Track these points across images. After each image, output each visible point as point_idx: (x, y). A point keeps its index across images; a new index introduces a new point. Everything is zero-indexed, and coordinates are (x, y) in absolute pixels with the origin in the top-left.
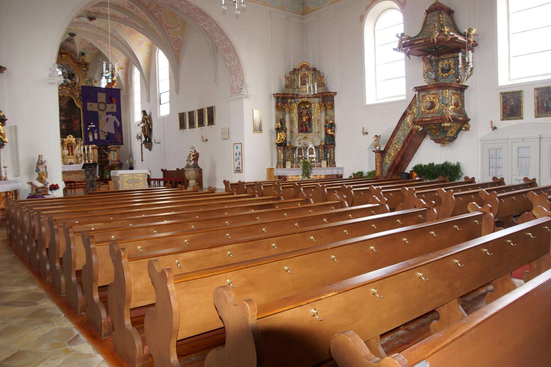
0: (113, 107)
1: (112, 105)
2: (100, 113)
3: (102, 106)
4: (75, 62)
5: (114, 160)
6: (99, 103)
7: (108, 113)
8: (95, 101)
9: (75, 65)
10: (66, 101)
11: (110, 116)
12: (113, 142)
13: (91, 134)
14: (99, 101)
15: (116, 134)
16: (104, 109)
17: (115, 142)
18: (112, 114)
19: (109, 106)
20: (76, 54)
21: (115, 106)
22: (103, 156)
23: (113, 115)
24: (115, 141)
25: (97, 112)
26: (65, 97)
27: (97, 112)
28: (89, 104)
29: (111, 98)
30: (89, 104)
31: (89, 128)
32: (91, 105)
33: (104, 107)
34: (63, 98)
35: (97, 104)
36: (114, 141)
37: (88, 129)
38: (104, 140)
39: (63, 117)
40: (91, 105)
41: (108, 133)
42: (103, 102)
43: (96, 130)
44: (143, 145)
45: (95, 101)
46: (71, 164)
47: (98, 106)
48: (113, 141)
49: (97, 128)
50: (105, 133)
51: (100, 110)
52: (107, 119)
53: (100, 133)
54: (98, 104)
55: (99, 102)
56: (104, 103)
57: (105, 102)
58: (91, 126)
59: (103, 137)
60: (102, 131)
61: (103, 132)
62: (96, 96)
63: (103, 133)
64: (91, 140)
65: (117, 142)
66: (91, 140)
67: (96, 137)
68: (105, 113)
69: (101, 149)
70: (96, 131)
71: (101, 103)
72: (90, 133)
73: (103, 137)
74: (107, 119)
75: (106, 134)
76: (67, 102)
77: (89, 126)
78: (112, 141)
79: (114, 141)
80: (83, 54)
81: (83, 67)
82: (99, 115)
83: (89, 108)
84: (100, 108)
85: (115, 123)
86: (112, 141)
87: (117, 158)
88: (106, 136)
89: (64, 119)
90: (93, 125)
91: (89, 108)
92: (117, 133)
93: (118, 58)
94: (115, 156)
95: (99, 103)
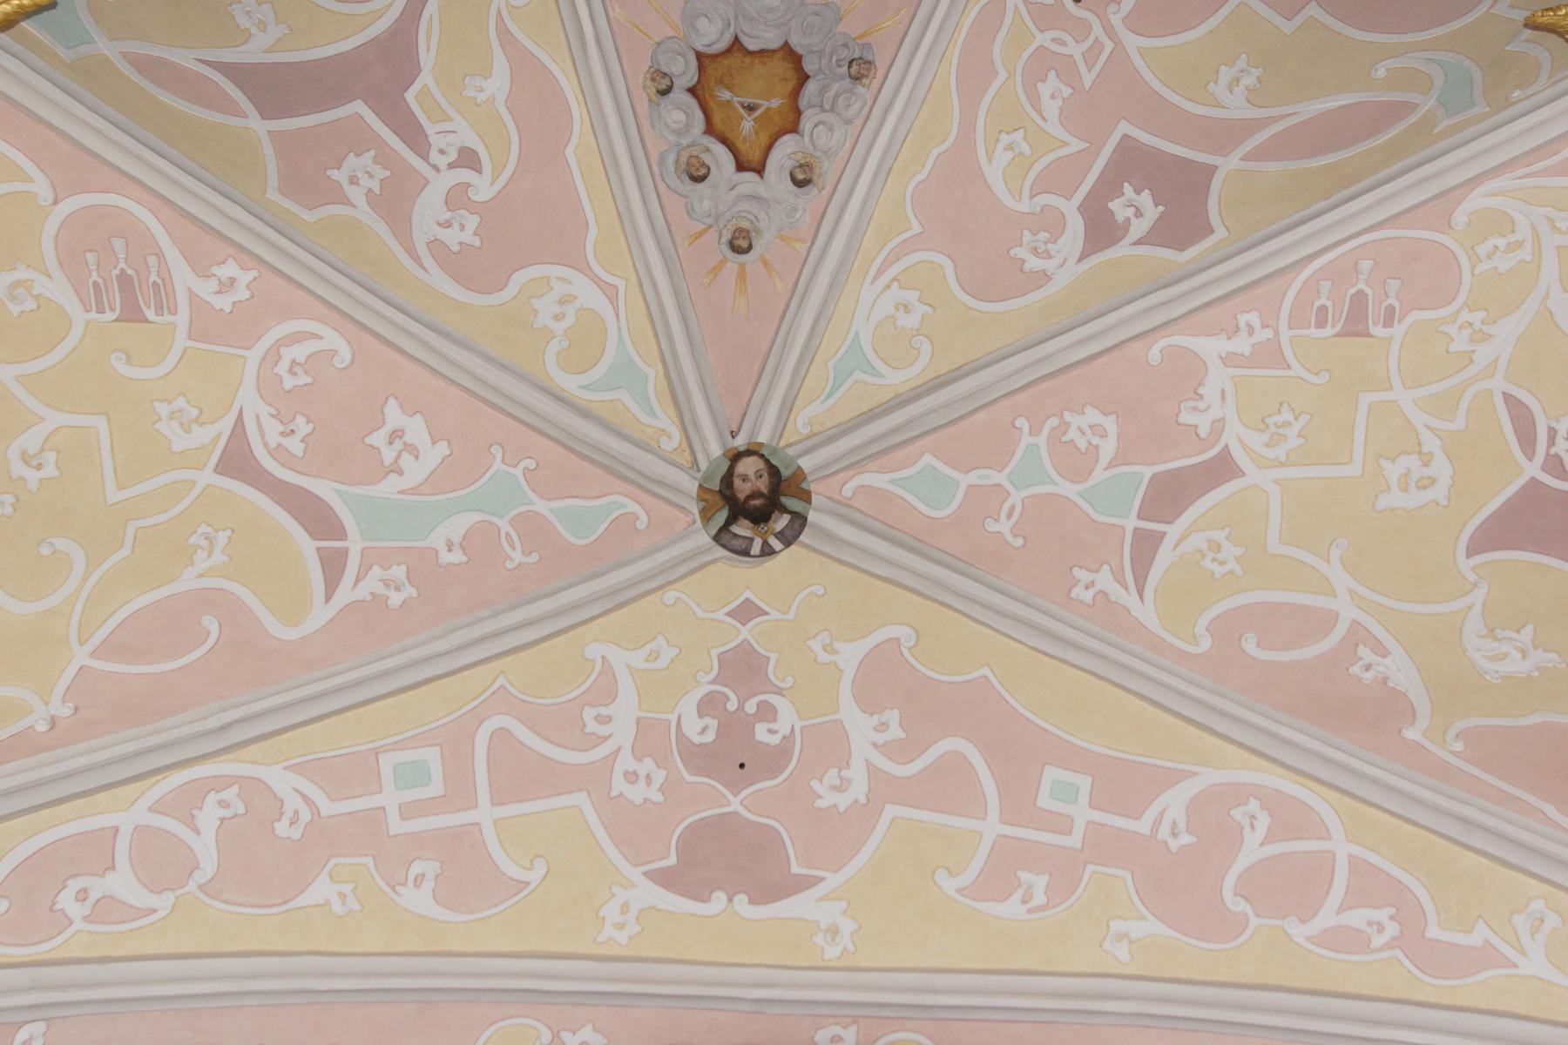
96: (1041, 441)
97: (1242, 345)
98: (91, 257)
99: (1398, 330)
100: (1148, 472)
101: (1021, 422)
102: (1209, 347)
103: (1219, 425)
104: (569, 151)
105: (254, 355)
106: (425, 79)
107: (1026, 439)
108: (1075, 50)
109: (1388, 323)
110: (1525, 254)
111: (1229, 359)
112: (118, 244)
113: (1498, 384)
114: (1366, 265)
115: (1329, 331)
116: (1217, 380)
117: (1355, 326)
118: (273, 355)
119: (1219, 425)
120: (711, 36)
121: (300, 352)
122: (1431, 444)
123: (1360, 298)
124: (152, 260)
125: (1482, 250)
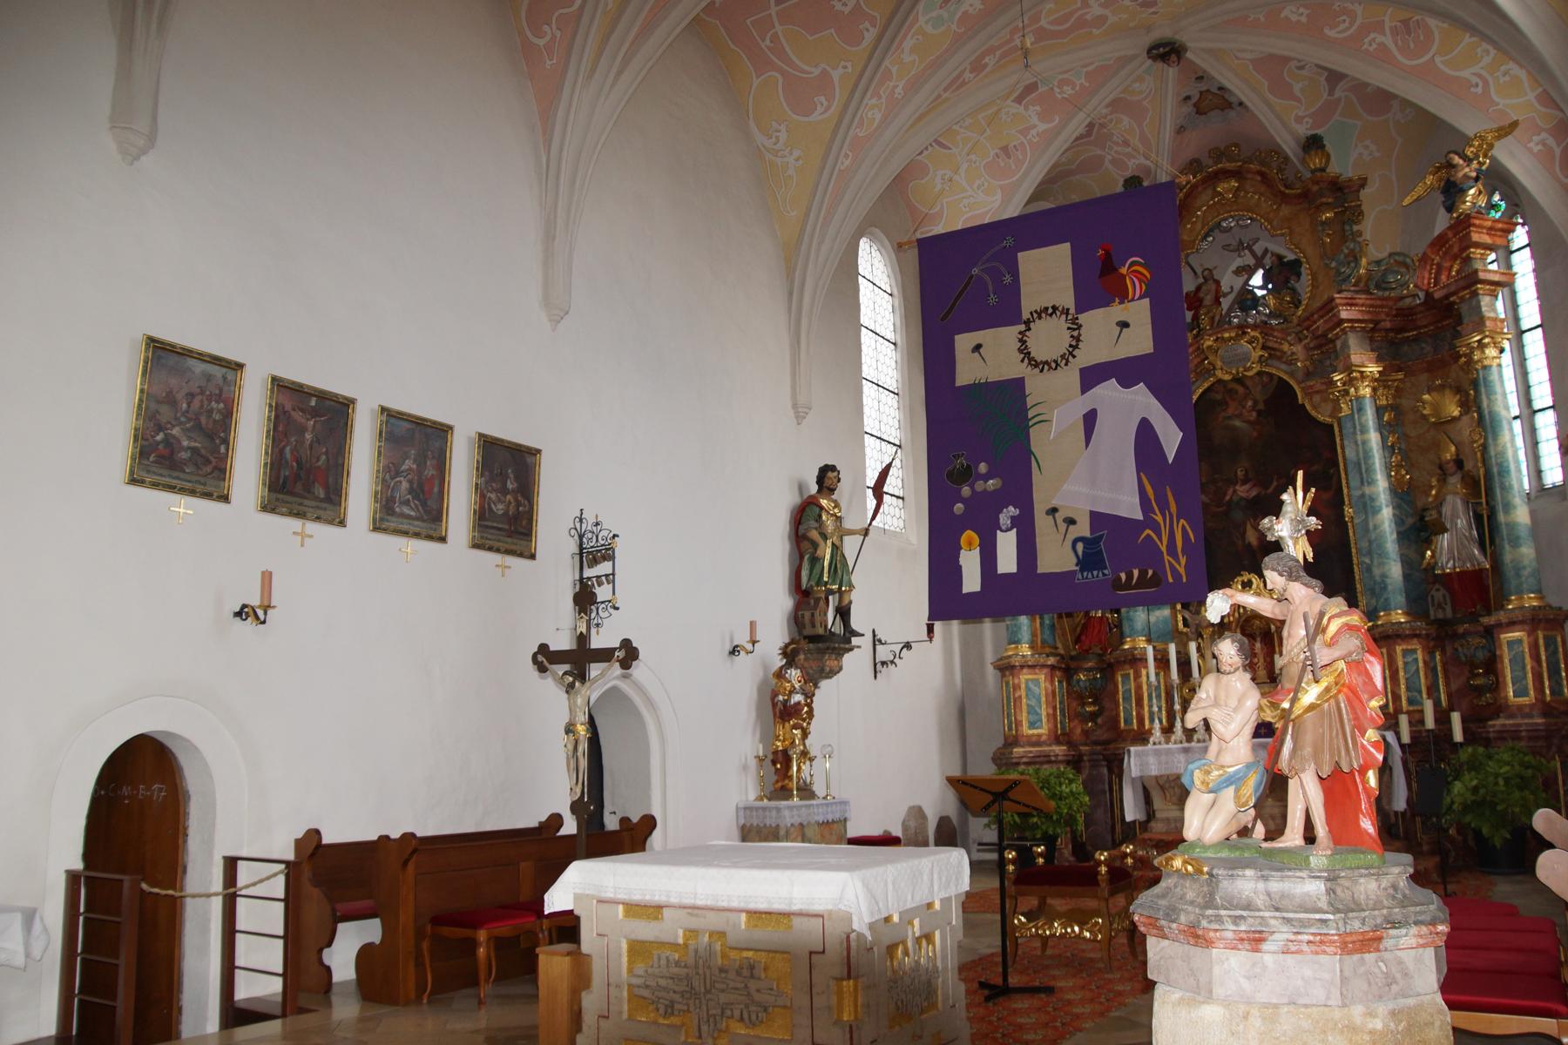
0: (1124, 325)
1: (1117, 311)
2: (1038, 387)
3: (1048, 338)
4: (1284, 199)
5: (1520, 707)
6: (1027, 323)
7: (1091, 377)
8: (1006, 310)
9: (1286, 210)
10: (1256, 402)
11: (1109, 391)
12: (1128, 585)
13: (977, 540)
14: (1028, 305)
15: (1149, 522)
16: (1056, 355)
17: (1139, 585)
18: (1126, 372)
19: (1097, 322)
20: (1287, 158)
21: (1139, 312)
22: (1479, 681)
23: (1126, 383)
24: (1143, 573)
25: (1019, 384)
26: (1249, 383)
27: (1019, 384)
28: (963, 342)
29: (1108, 267)
30: (963, 342)
31: (963, 500)
32: (978, 348)
33: (1066, 340)
34: (1241, 390)
35: (1012, 332)
36: (1136, 573)
37: (959, 508)
38: (1073, 573)
39: (1247, 487)
40: (978, 348)
41: (1097, 518)
42: (1055, 308)
43: (1012, 511)
44: (851, 569)
45: (1006, 310)
46: (1263, 731)
47: (1023, 342)
48: (1130, 576)
49: (1019, 490)
50: (1071, 521)
51: (1036, 366)
52: (1090, 419)
53: (1042, 522)
54: (1022, 327)
55: (1026, 315)
56: (1067, 311)
57: (1068, 300)
58: (979, 486)
59: (1056, 556)
60: (1053, 511)
61: (1060, 516)
62: (1008, 279)
63: (1063, 526)
64: (972, 581)
65: (1157, 581)
66: (972, 581)
67: (1007, 561)
68: (1070, 377)
69: (1455, 636)
70: (1004, 519)
71: (1042, 313)
72: (969, 535)
73: (1056, 556)
74: (1090, 419)
75: (1084, 529)
76: (1261, 406)
77: (966, 491)
78: (1123, 576)
79: (1136, 573)
80: (1313, 144)
81: (1320, 208)
82: (1030, 401)
83: (968, 372)
84: (1039, 353)
85: (1146, 435)
86: (1123, 576)
87: (1539, 688)
88: (1080, 547)
89: (1254, 493)
90: (986, 478)
91: (968, 372)
92: (1164, 507)
93: (1486, 83)
94: (1525, 677)
95: (1027, 323)
96: (1078, 83)
97: (1034, 132)
98: (1422, 38)
99: (992, 153)
100: (1040, 90)
101: (1087, 85)
102: (1042, 127)
103: (1026, 108)
104: (1266, 83)
105: (1358, 23)
106: (1323, 79)
107: (1083, 81)
108: (1115, 148)
109: (997, 154)
110: (975, 187)
111: (1035, 126)
112: (1412, 46)
113: (954, 150)
114: (1013, 167)
115: (1012, 145)
116: (1035, 120)
117: (1005, 149)
118: (1352, 24)
119: (1026, 108)
120: (1232, 114)
121: (1342, 27)
122: (963, 130)
123: (1009, 158)
124: (1400, 43)
125: (986, 184)
